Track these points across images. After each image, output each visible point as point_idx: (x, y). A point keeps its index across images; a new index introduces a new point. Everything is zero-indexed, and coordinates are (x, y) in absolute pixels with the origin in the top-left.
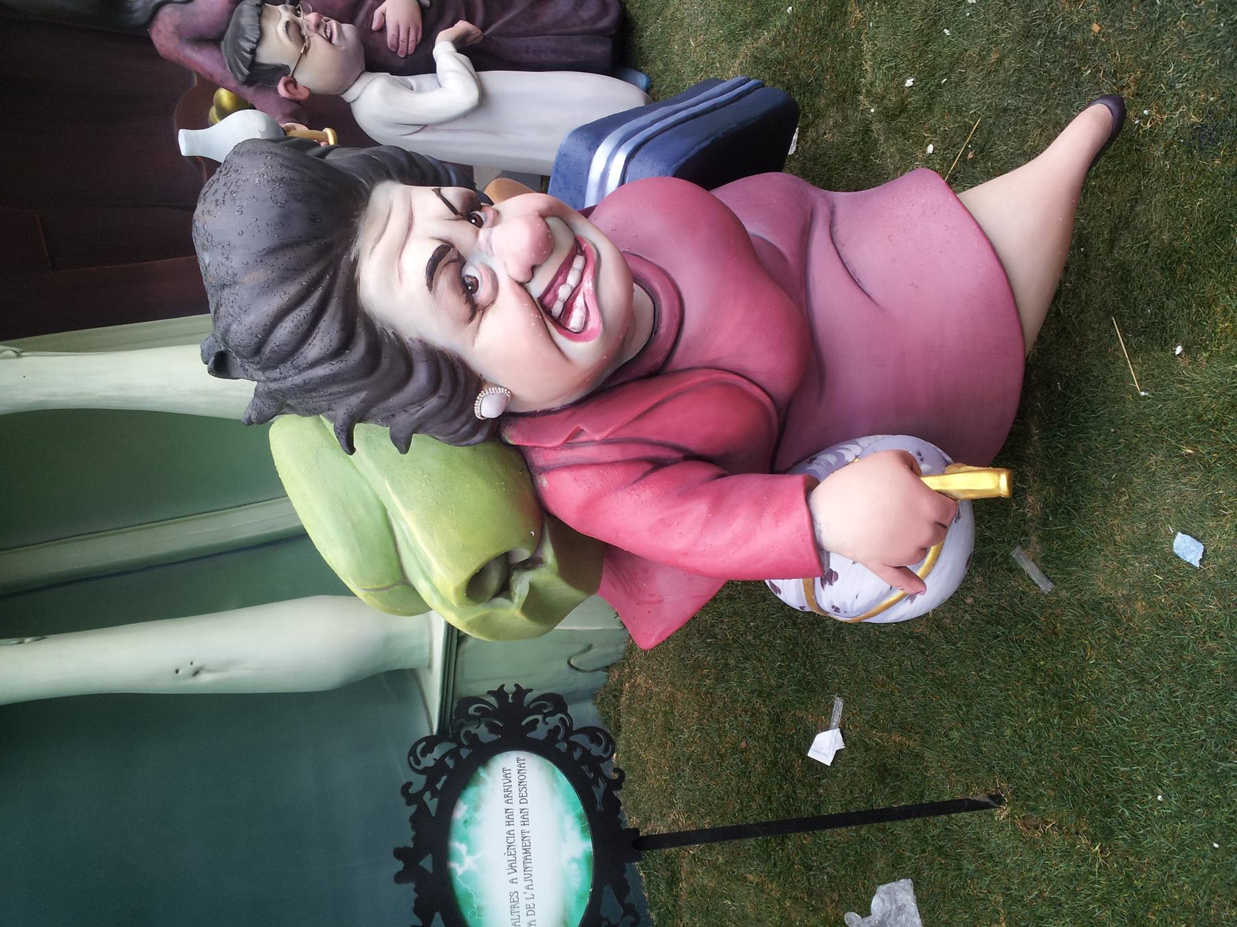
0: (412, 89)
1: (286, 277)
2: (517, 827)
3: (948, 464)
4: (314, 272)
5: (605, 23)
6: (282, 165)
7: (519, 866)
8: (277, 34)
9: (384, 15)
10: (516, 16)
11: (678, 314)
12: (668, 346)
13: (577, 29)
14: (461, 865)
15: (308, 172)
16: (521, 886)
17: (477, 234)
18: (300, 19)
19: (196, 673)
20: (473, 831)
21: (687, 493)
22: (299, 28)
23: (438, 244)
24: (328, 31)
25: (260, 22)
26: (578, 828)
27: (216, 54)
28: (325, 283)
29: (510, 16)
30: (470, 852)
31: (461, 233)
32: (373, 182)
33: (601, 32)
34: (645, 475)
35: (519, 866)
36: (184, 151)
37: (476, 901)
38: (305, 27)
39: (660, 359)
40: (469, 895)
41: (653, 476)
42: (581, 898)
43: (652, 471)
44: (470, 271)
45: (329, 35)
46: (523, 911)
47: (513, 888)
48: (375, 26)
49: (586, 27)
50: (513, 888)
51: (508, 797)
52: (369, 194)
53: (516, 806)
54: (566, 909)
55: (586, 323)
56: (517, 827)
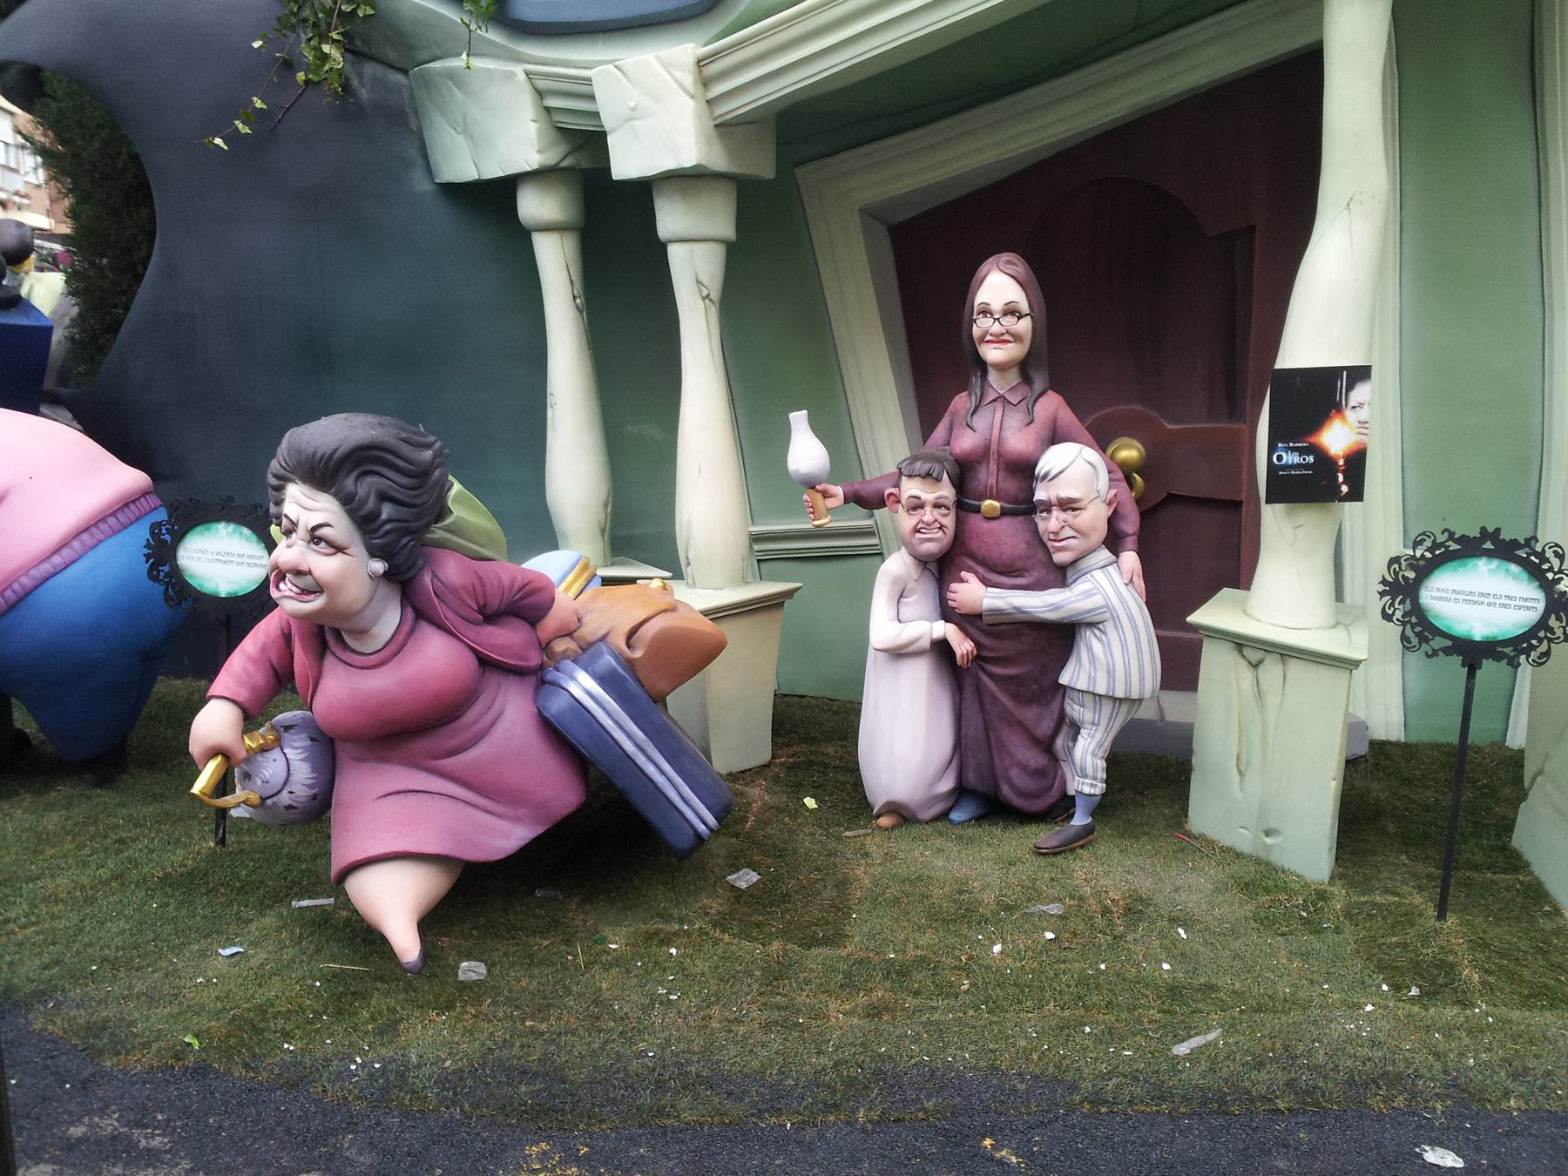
0: (901, 596)
1: (289, 451)
2: (236, 559)
3: (263, 799)
4: (290, 464)
5: (1006, 790)
6: (325, 453)
7: (219, 557)
8: (910, 489)
9: (967, 582)
10: (1003, 704)
11: (355, 664)
12: (338, 654)
13: (997, 761)
14: (225, 528)
15: (322, 463)
16: (210, 556)
17: (302, 540)
18: (928, 509)
19: (552, 406)
20: (237, 535)
21: (264, 649)
22: (922, 506)
23: (294, 520)
24: (924, 531)
25: (916, 476)
26: (232, 591)
27: (941, 441)
28: (288, 468)
29: (1004, 699)
30: (228, 533)
31: (301, 531)
32: (335, 495)
33: (997, 787)
34: (282, 630)
35: (219, 557)
36: (792, 415)
37: (206, 532)
38: (923, 511)
39: (332, 649)
40: (209, 530)
41: (279, 632)
42: (200, 585)
43: (284, 634)
44: (294, 535)
45: (921, 530)
46: (200, 555)
47: (210, 553)
48: (963, 574)
49: (999, 770)
50: (210, 553)
51: (250, 557)
52: (325, 492)
53: (245, 560)
54: (197, 578)
55: (280, 591)
56: (236, 559)
